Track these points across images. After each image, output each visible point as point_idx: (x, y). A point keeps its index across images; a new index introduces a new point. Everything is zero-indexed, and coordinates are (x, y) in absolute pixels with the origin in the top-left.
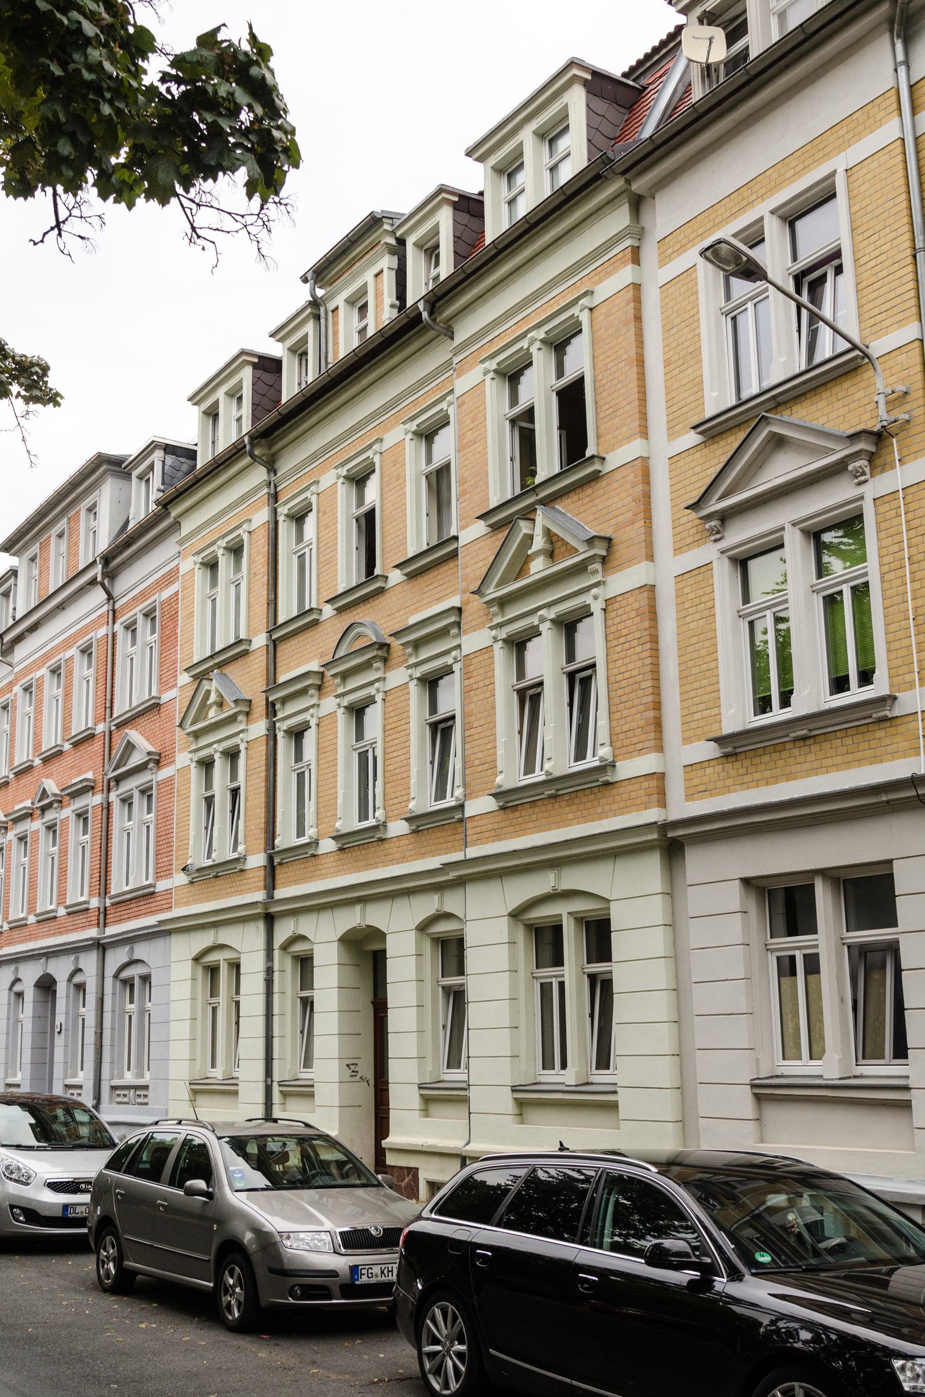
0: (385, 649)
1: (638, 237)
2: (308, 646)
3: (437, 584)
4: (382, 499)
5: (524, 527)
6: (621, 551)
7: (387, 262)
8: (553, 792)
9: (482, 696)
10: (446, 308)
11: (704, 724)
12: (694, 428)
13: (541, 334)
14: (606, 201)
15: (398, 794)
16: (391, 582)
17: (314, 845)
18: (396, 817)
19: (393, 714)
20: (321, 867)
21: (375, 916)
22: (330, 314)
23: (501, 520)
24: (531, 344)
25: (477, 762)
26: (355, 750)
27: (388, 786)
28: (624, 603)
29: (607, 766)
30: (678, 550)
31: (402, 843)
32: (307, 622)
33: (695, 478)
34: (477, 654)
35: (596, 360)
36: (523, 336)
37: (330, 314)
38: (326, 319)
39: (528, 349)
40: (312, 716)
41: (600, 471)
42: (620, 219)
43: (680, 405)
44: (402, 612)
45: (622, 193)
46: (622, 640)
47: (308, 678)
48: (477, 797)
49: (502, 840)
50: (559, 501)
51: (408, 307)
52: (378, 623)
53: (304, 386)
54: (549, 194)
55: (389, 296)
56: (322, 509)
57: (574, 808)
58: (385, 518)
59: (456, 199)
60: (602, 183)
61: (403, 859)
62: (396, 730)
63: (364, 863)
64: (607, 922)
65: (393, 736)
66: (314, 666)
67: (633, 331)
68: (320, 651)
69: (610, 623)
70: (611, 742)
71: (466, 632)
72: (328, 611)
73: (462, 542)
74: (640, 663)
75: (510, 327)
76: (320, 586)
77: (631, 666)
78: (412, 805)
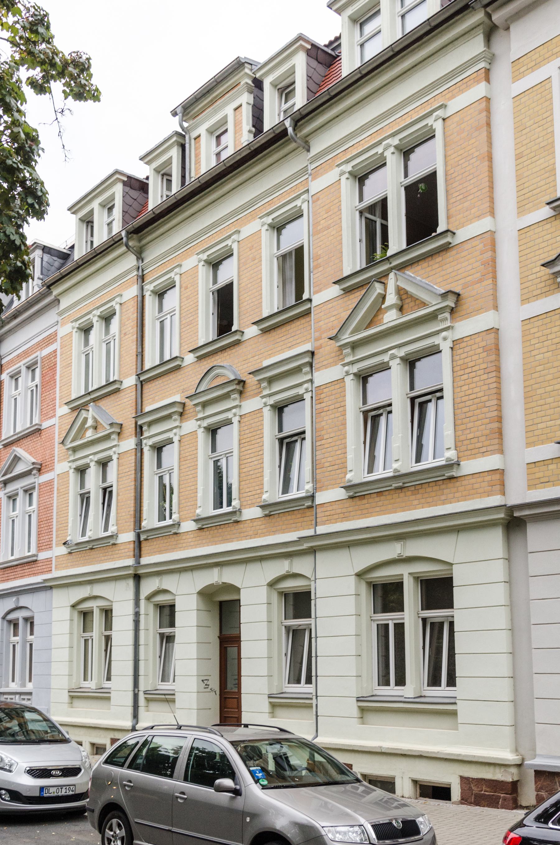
0: (242, 384)
1: (489, 61)
2: (171, 385)
3: (289, 336)
4: (239, 276)
5: (378, 288)
6: (468, 303)
7: (246, 99)
8: (401, 484)
9: (333, 416)
10: (305, 127)
11: (549, 431)
12: (548, 204)
13: (395, 141)
14: (463, 32)
15: (252, 489)
16: (246, 336)
17: (177, 526)
18: (251, 505)
19: (247, 431)
20: (182, 541)
21: (230, 576)
22: (193, 141)
23: (351, 285)
24: (385, 149)
25: (327, 464)
26: (211, 458)
27: (243, 483)
28: (470, 343)
29: (451, 465)
30: (525, 300)
31: (255, 524)
32: (170, 368)
33: (545, 244)
34: (328, 385)
35: (448, 158)
36: (379, 143)
37: (193, 141)
38: (190, 145)
39: (383, 153)
40: (175, 434)
41: (450, 243)
42: (476, 46)
43: (531, 188)
44: (256, 358)
45: (478, 26)
46: (469, 370)
47: (173, 407)
48: (327, 489)
49: (350, 520)
50: (409, 268)
51: (265, 131)
52: (233, 366)
53: (165, 198)
54: (401, 36)
55: (248, 124)
56: (184, 285)
57: (419, 496)
58: (241, 289)
59: (309, 47)
60: (470, 12)
61: (256, 535)
62: (250, 443)
63: (220, 539)
64: (450, 579)
65: (248, 448)
66: (177, 398)
67: (485, 134)
68: (182, 388)
69: (456, 358)
70: (456, 447)
71: (318, 369)
72: (190, 358)
73: (314, 303)
74: (486, 387)
75: (365, 140)
76: (182, 341)
77: (477, 390)
78: (265, 496)
